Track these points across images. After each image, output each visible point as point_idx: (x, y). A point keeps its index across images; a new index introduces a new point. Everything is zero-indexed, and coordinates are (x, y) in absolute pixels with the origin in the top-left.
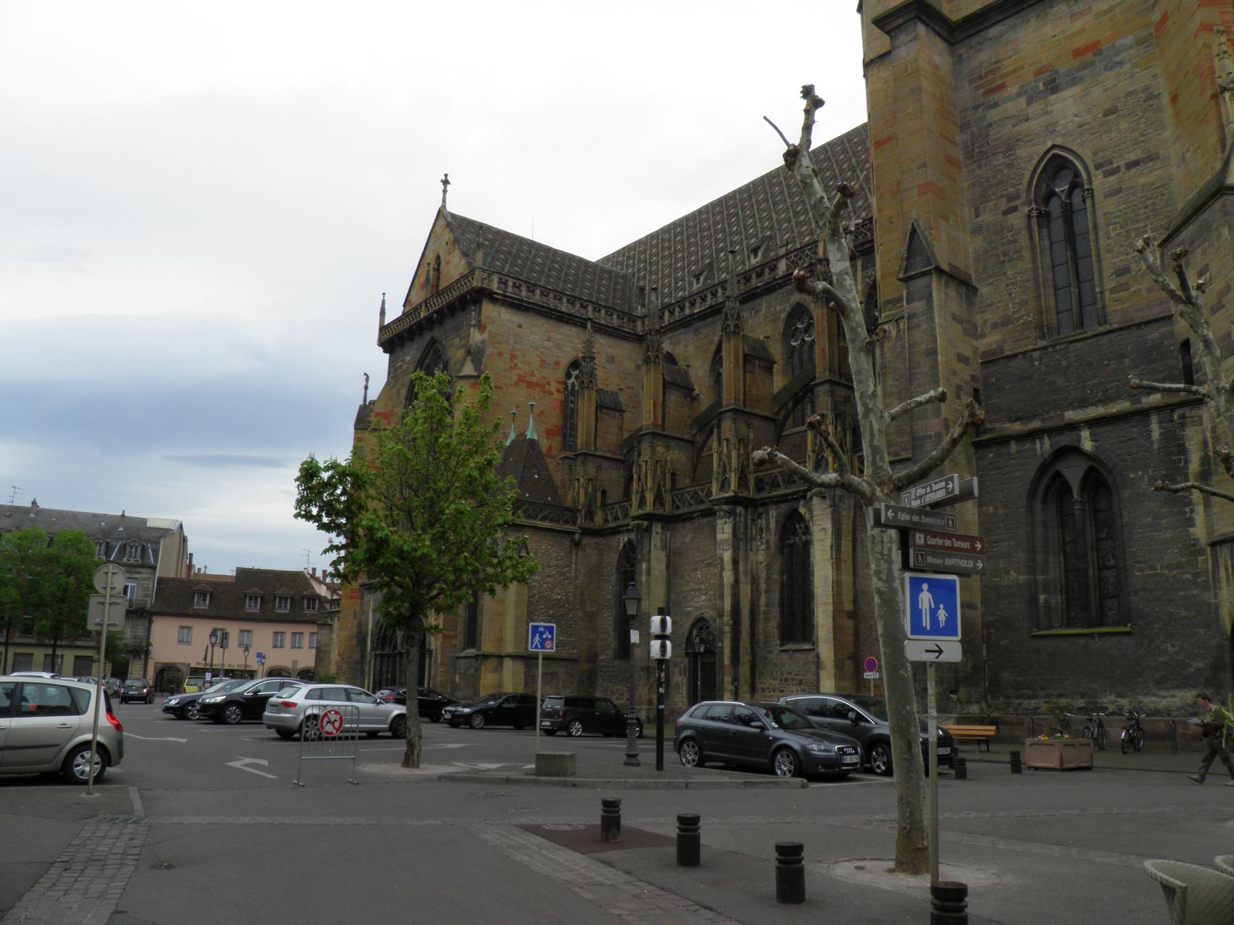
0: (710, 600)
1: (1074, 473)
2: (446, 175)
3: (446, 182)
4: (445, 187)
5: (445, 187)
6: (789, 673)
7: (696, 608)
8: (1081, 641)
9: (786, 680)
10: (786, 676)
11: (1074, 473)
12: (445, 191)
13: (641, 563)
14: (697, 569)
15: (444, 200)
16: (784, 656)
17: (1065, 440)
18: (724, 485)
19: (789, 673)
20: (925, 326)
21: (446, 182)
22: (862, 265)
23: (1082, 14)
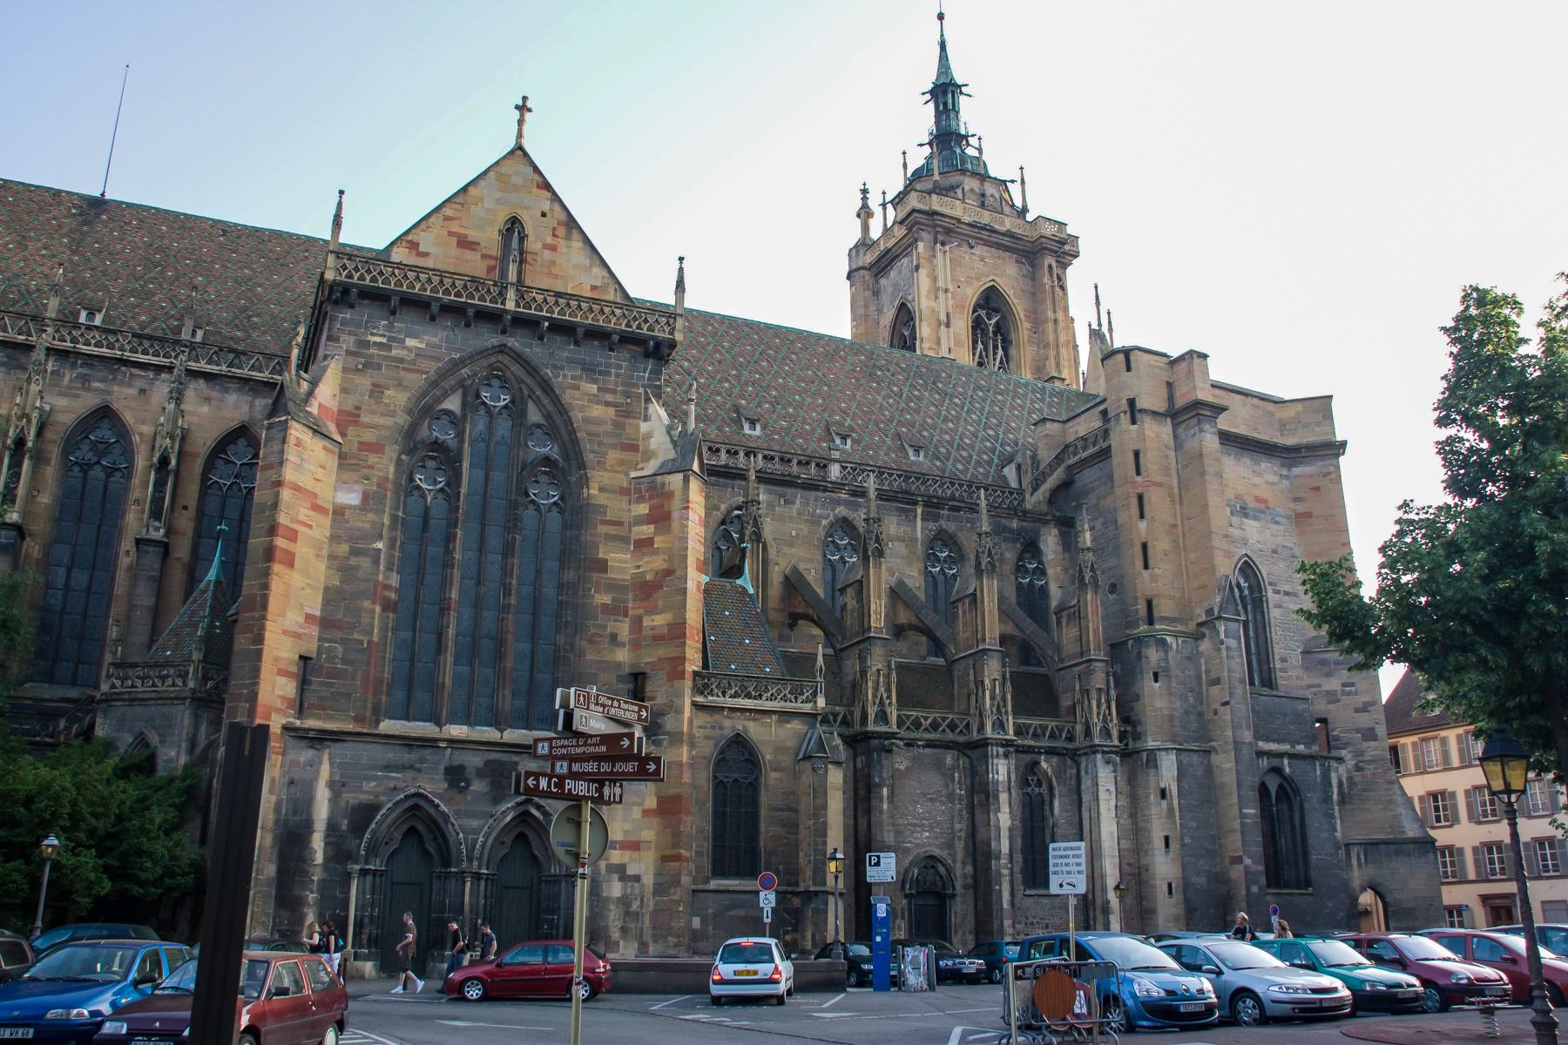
0: (936, 838)
1: (1273, 785)
2: (525, 98)
3: (523, 108)
4: (522, 116)
5: (522, 116)
6: (1034, 917)
7: (917, 845)
8: (1289, 898)
9: (1032, 924)
10: (1031, 920)
11: (1273, 785)
12: (521, 122)
13: (880, 786)
14: (917, 802)
15: (520, 135)
16: (1029, 901)
17: (1275, 762)
18: (1000, 725)
19: (1034, 917)
20: (1238, 660)
21: (523, 108)
22: (922, 515)
23: (1259, 475)
